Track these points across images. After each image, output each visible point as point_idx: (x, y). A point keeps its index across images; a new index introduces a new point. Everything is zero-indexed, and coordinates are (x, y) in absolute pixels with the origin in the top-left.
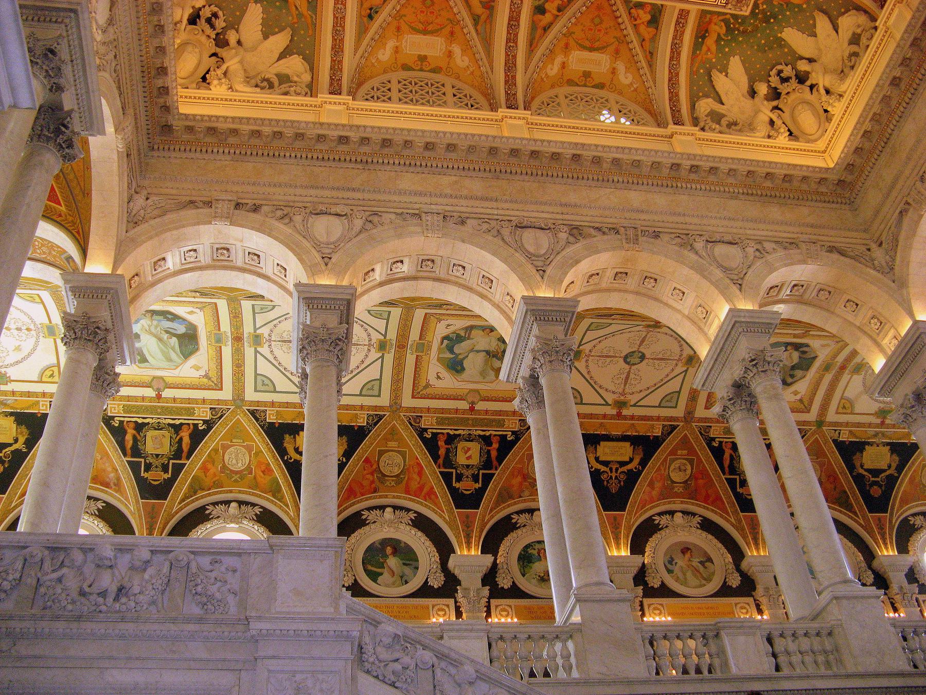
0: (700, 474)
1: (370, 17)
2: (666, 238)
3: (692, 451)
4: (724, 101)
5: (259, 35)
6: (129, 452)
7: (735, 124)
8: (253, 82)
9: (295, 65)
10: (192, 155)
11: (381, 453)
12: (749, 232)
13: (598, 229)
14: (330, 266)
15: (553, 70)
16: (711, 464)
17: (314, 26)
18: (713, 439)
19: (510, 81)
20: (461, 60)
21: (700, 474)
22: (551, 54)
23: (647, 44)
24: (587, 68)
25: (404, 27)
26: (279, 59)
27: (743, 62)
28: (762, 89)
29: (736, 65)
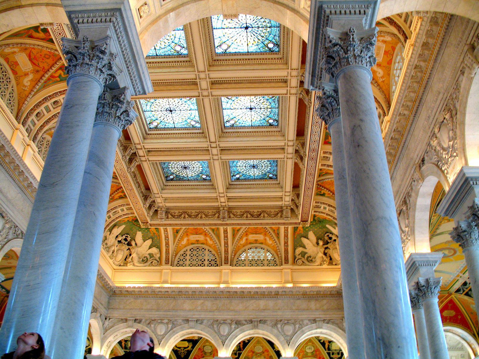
0: (317, 350)
1: (177, 232)
2: (268, 322)
3: (313, 343)
4: (306, 247)
5: (142, 241)
6: (124, 348)
7: (310, 257)
8: (141, 259)
9: (154, 250)
10: (122, 298)
11: (204, 346)
12: (299, 316)
13: (246, 321)
14: (161, 345)
15: (243, 241)
16: (320, 347)
17: (159, 236)
18: (321, 340)
19: (226, 251)
20: (210, 242)
21: (317, 350)
22: (241, 238)
23: (276, 231)
24: (256, 239)
25: (189, 234)
26: (149, 249)
27: (314, 233)
28: (321, 243)
29: (311, 235)
